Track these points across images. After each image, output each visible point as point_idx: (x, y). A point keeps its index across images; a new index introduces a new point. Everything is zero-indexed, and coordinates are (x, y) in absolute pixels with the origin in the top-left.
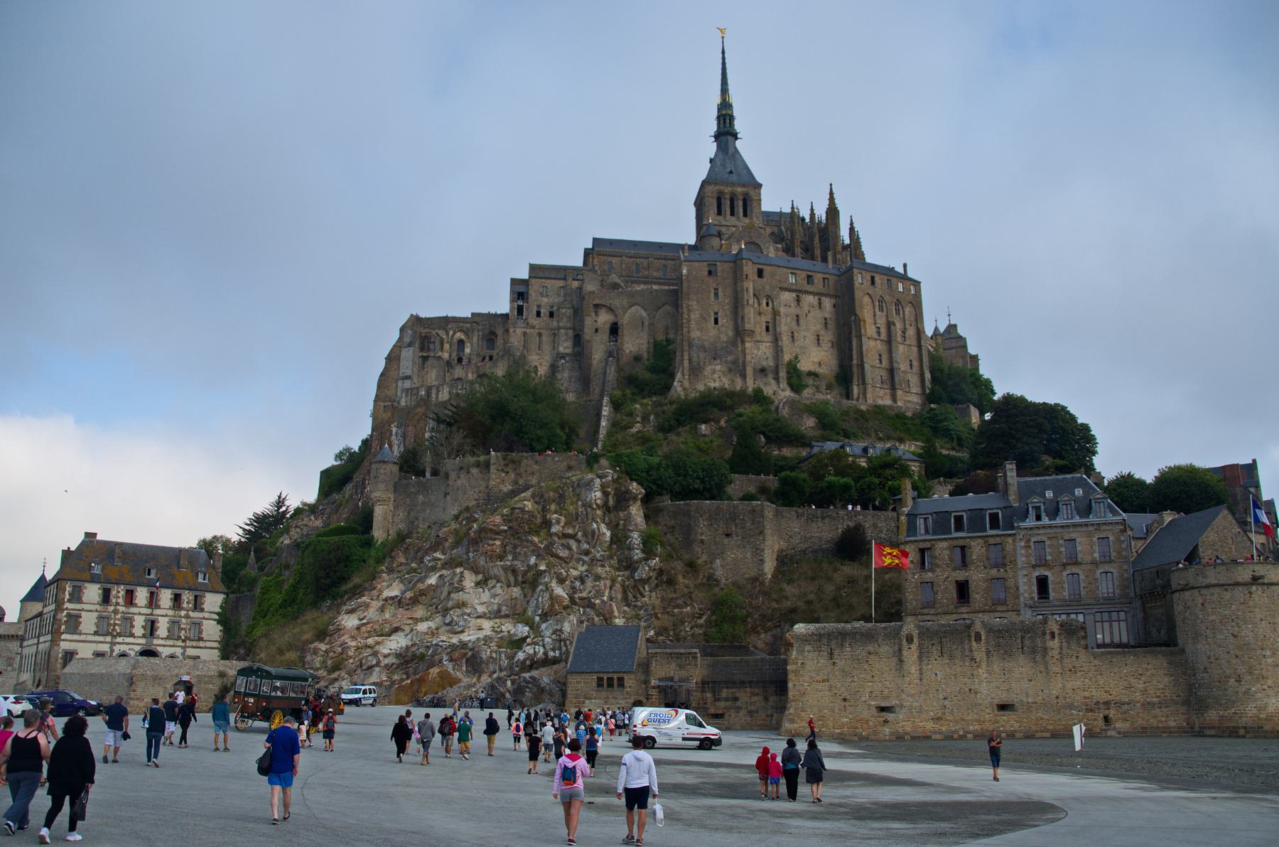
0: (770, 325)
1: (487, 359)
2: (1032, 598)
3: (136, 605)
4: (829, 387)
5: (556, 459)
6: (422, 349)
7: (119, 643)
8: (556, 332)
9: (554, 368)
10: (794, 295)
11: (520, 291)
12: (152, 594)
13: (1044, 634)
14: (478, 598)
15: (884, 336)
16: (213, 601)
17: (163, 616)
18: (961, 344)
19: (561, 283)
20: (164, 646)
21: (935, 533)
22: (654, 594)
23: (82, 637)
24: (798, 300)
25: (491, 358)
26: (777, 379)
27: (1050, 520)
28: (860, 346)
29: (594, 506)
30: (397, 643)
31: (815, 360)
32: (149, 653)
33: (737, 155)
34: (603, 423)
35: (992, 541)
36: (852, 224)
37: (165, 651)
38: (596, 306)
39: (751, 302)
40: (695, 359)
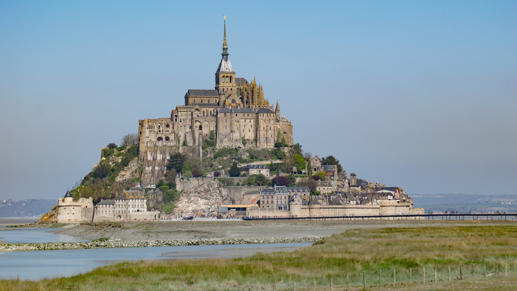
0: (239, 128)
4: (252, 143)
9: (185, 136)
10: (244, 120)
14: (201, 201)
15: (265, 129)
16: (145, 201)
19: (186, 113)
25: (168, 131)
26: (240, 142)
30: (190, 209)
32: (138, 211)
34: (201, 154)
37: (140, 210)
38: (196, 121)
40: (221, 138)
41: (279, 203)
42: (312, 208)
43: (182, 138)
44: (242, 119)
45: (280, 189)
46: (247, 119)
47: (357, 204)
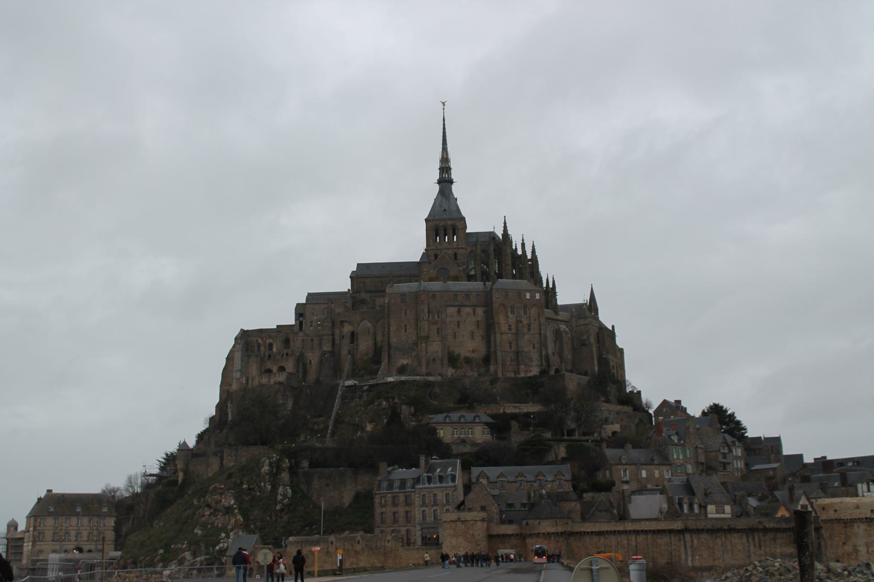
0: (440, 330)
1: (285, 355)
2: (420, 521)
3: (71, 526)
5: (254, 449)
6: (247, 350)
7: (64, 545)
8: (322, 337)
9: (321, 362)
10: (456, 308)
11: (301, 311)
12: (78, 519)
13: (385, 541)
15: (513, 331)
16: (111, 522)
17: (85, 530)
18: (587, 322)
19: (326, 306)
20: (85, 545)
21: (387, 490)
22: (285, 517)
23: (46, 543)
24: (459, 312)
25: (287, 354)
27: (429, 484)
28: (495, 340)
29: (264, 474)
31: (471, 349)
33: (451, 196)
35: (407, 494)
36: (523, 240)
37: (86, 548)
38: (342, 322)
39: (425, 319)
41: (430, 519)
42: (531, 535)
43: (314, 367)
44: (448, 306)
45: (438, 470)
46: (464, 306)
47: (737, 516)
